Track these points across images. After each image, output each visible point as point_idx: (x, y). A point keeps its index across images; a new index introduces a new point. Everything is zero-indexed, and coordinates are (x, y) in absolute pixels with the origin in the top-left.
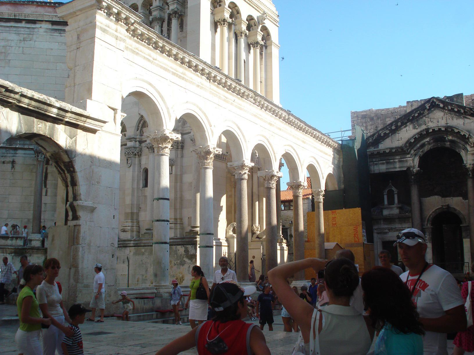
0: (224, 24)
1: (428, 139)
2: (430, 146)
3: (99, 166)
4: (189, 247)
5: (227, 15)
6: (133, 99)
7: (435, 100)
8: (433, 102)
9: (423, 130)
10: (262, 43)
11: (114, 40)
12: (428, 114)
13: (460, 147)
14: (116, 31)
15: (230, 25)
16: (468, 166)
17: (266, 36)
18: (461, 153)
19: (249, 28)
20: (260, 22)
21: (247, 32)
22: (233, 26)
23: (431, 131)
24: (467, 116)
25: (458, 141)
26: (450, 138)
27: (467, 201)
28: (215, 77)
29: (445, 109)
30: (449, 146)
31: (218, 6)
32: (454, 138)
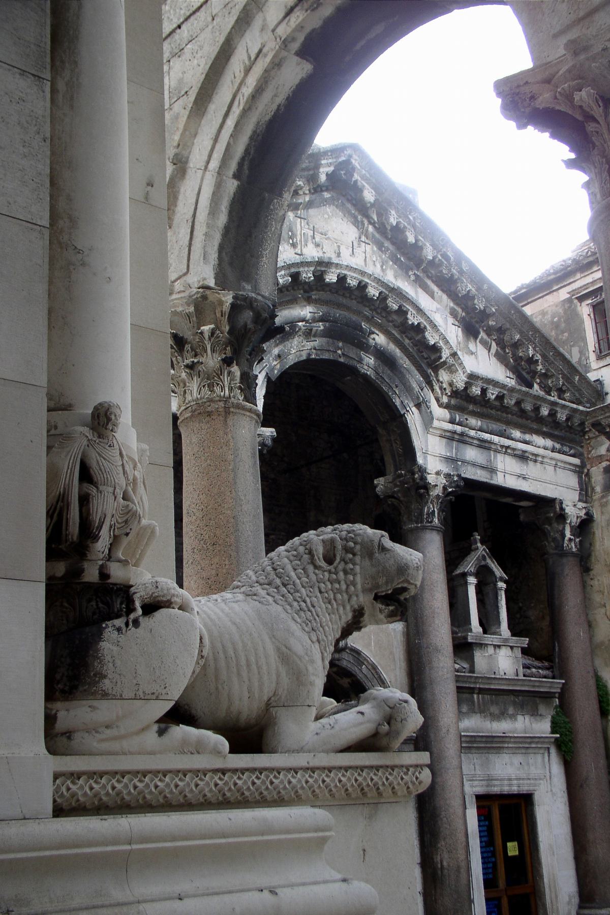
1: (306, 311)
2: (309, 345)
7: (355, 162)
8: (347, 162)
9: (308, 264)
12: (309, 205)
13: (408, 389)
16: (431, 479)
18: (409, 417)
23: (331, 278)
24: (429, 282)
25: (405, 362)
26: (380, 339)
27: (398, 627)
29: (368, 217)
30: (370, 372)
32: (393, 348)
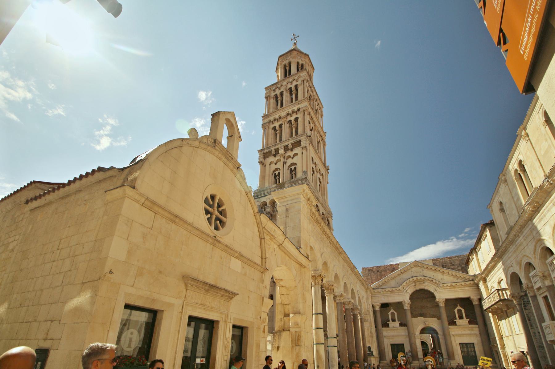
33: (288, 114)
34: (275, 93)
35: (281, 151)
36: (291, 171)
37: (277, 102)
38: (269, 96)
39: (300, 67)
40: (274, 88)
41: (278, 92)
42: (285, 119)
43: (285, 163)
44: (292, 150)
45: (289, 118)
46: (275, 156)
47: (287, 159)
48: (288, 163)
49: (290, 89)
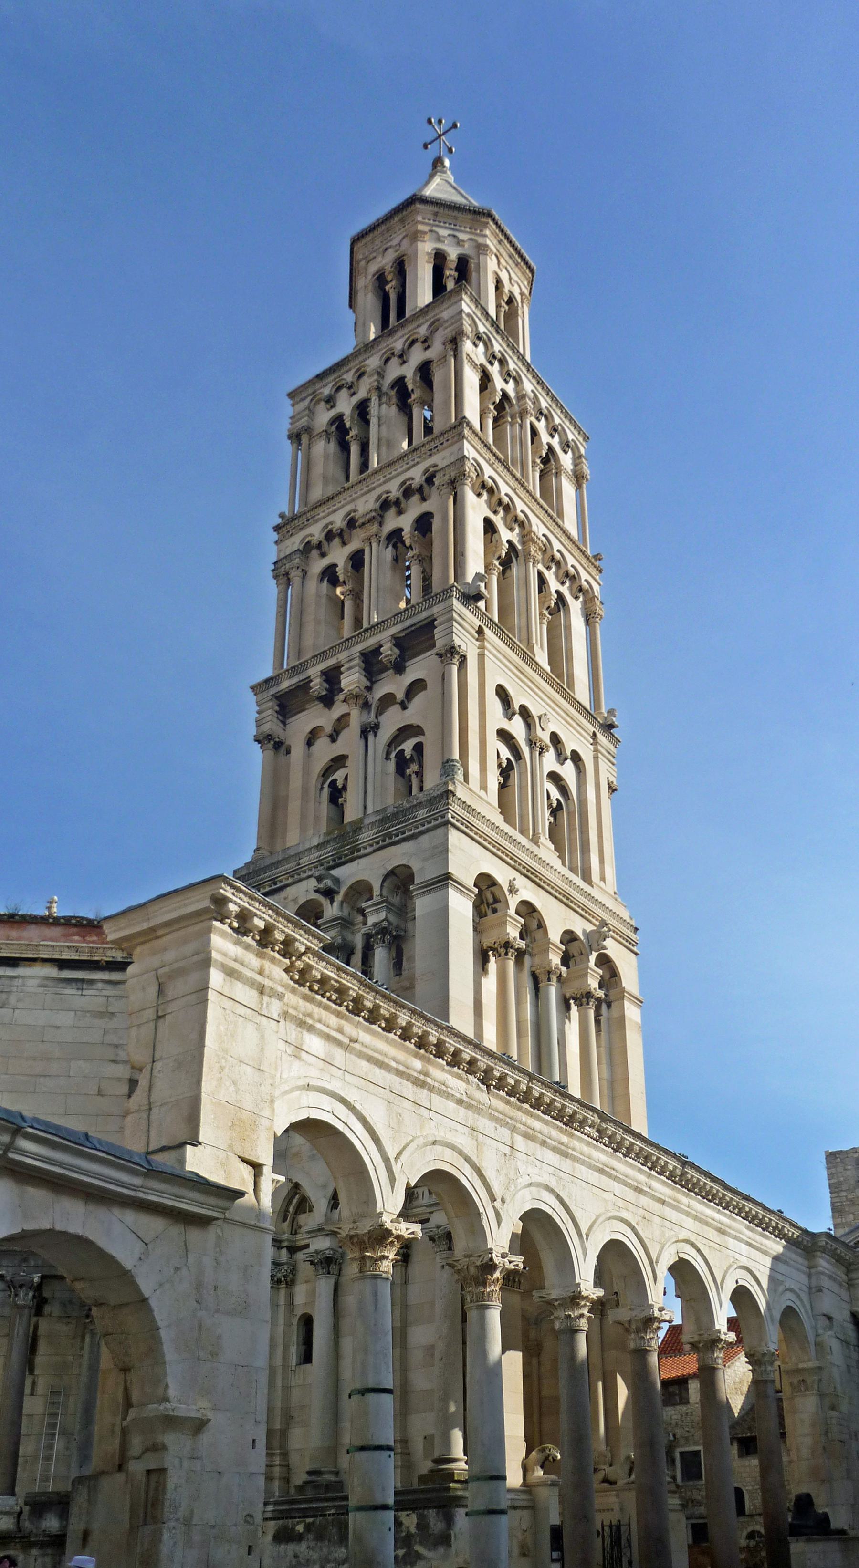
0: (506, 954)
3: (217, 1311)
4: (431, 1514)
5: (513, 932)
6: (298, 1140)
10: (601, 994)
11: (254, 993)
14: (261, 973)
15: (520, 955)
17: (607, 977)
19: (566, 960)
20: (595, 946)
21: (564, 969)
22: (527, 957)
28: (502, 1078)
31: (489, 912)
33: (385, 505)
34: (333, 413)
35: (352, 680)
36: (402, 764)
37: (344, 447)
38: (308, 430)
39: (450, 273)
40: (326, 391)
41: (345, 405)
42: (374, 528)
43: (368, 731)
44: (399, 668)
45: (392, 522)
46: (328, 701)
47: (380, 712)
48: (387, 731)
49: (400, 383)
